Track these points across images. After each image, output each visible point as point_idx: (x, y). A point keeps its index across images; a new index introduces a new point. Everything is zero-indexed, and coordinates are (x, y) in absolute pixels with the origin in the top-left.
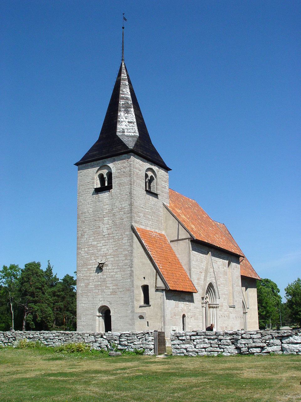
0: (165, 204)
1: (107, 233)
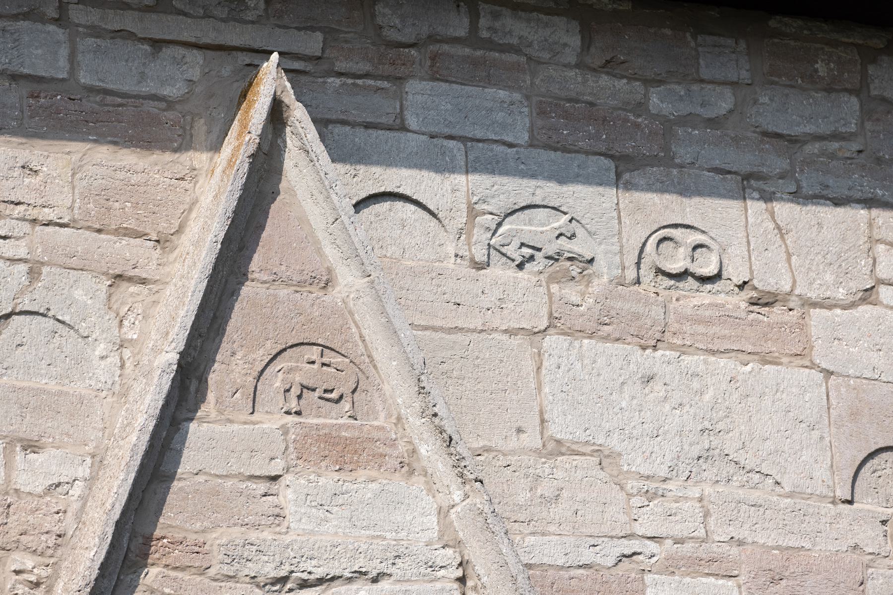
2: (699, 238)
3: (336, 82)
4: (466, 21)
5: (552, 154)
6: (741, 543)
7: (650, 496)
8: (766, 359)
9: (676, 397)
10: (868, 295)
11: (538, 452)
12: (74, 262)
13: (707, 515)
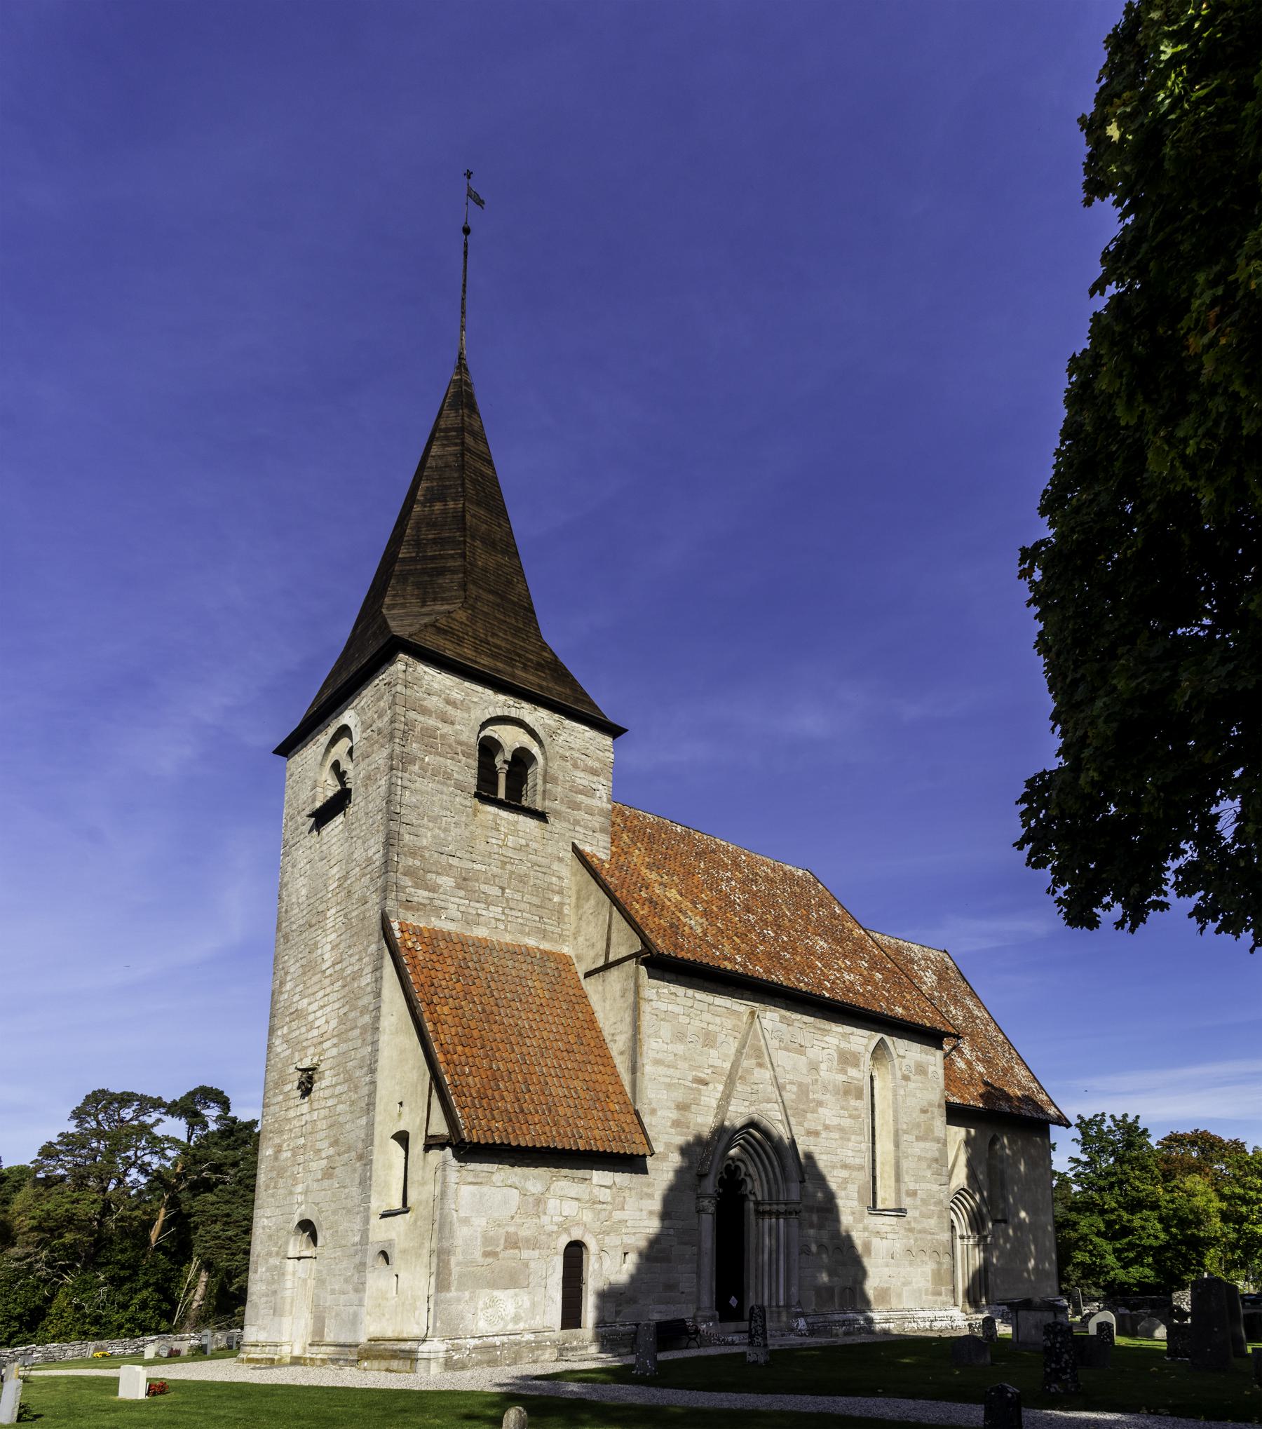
0: (587, 849)
1: (328, 964)
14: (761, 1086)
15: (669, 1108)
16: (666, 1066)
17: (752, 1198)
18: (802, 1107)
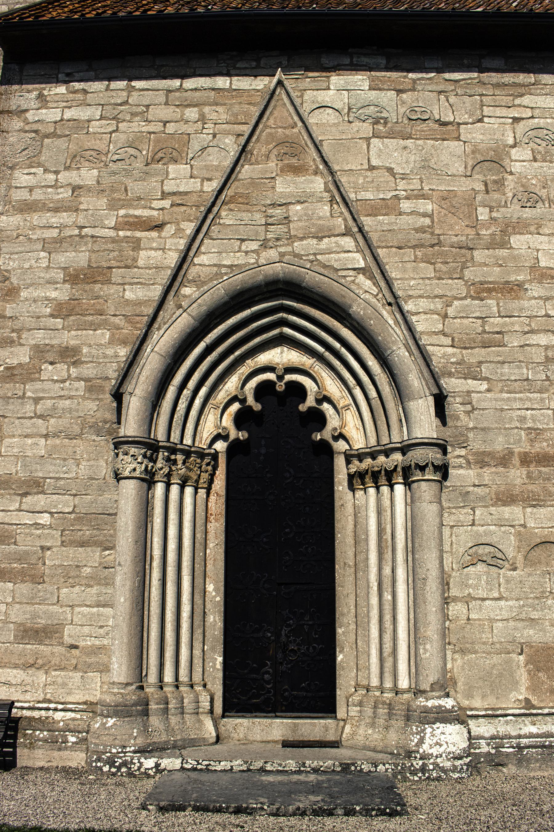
2: (424, 109)
3: (309, 80)
4: (349, 60)
5: (376, 92)
6: (433, 190)
7: (403, 179)
8: (444, 140)
9: (414, 152)
10: (480, 121)
11: (367, 170)
12: (226, 132)
13: (422, 182)
14: (298, 207)
15: (52, 282)
16: (49, 210)
17: (341, 446)
18: (455, 239)
